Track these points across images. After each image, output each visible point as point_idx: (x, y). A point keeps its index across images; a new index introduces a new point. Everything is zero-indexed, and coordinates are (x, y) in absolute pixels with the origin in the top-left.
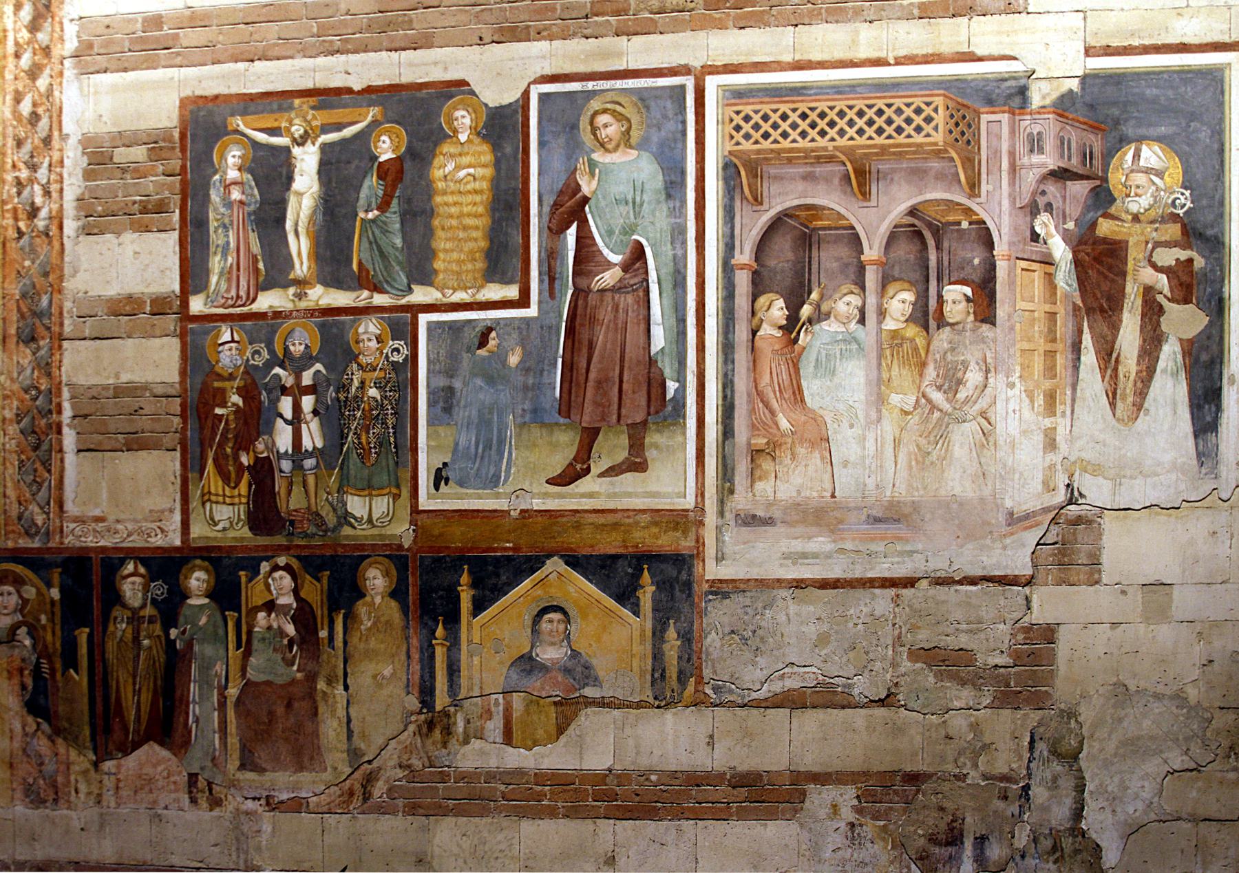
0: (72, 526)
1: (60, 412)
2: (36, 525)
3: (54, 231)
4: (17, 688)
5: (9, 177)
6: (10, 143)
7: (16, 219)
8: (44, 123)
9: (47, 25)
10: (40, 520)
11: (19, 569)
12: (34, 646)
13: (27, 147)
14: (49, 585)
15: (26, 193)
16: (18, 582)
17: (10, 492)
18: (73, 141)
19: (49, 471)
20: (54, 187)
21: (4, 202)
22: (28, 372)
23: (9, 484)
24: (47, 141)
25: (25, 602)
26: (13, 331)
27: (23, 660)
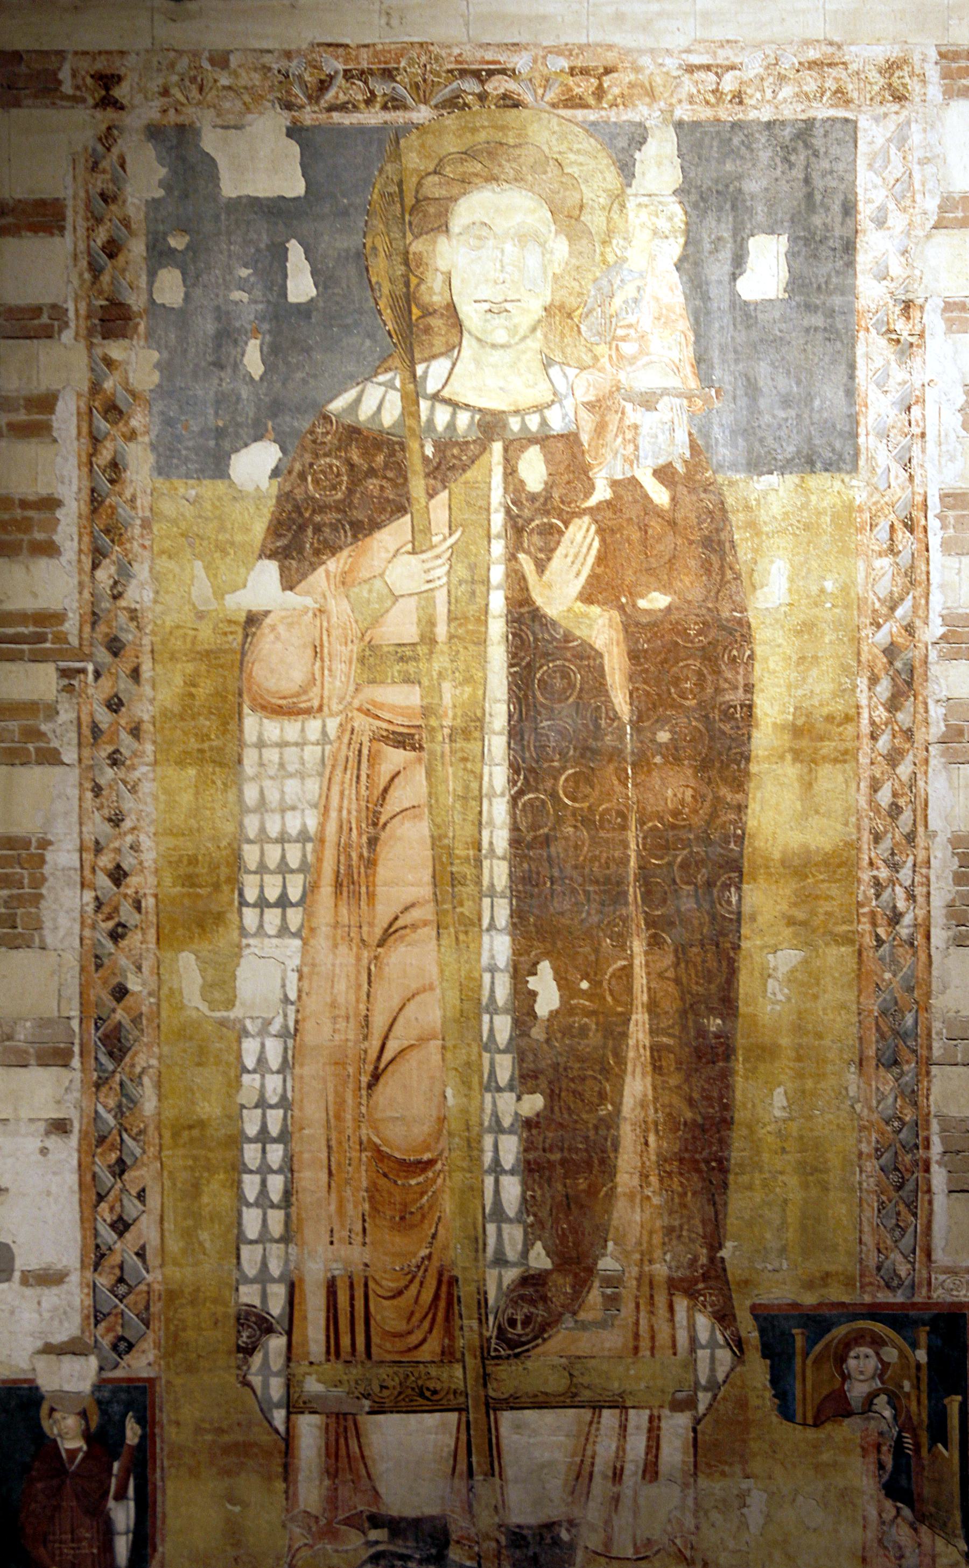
0: (942, 1277)
1: (927, 1147)
2: (899, 1277)
3: (919, 940)
4: (873, 1467)
5: (866, 876)
6: (866, 837)
7: (874, 924)
8: (906, 816)
9: (909, 704)
10: (903, 1270)
11: (879, 1328)
12: (895, 1417)
13: (887, 843)
14: (914, 1345)
15: (886, 895)
16: (877, 1342)
17: (867, 1238)
18: (941, 839)
19: (915, 1215)
20: (919, 891)
21: (860, 905)
22: (890, 1100)
23: (866, 1229)
24: (911, 838)
25: (885, 1365)
26: (871, 1052)
27: (881, 1434)
